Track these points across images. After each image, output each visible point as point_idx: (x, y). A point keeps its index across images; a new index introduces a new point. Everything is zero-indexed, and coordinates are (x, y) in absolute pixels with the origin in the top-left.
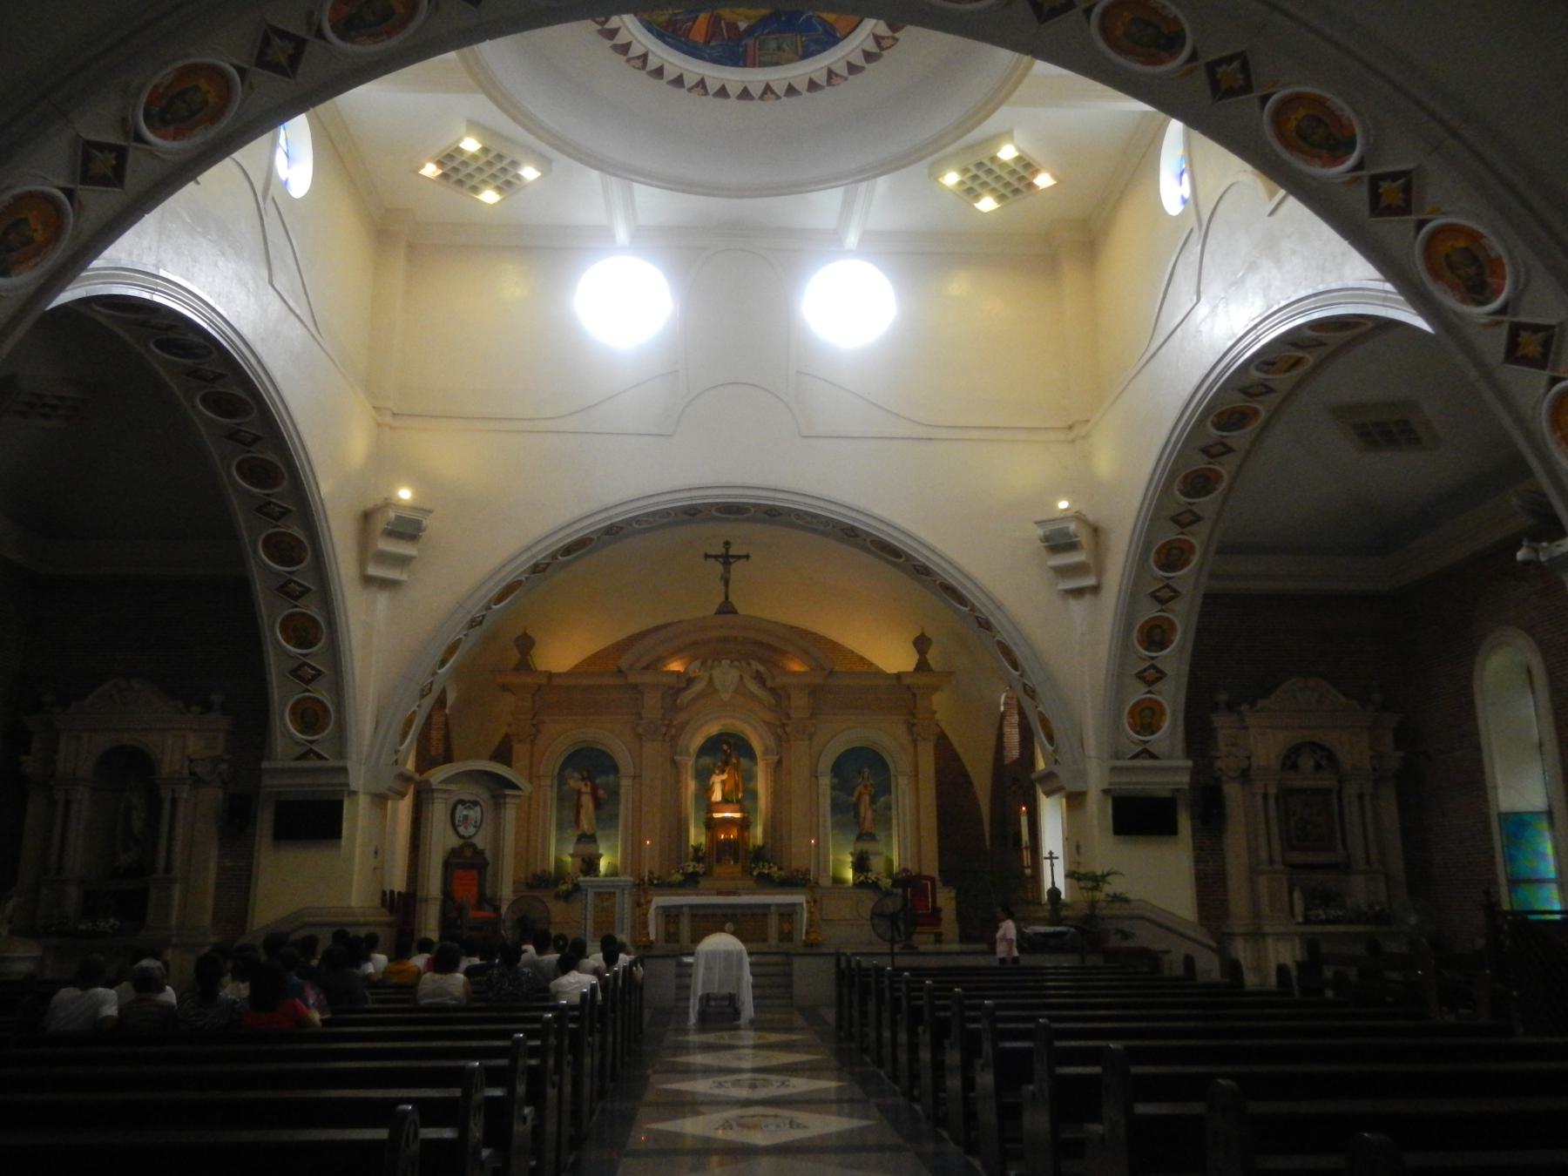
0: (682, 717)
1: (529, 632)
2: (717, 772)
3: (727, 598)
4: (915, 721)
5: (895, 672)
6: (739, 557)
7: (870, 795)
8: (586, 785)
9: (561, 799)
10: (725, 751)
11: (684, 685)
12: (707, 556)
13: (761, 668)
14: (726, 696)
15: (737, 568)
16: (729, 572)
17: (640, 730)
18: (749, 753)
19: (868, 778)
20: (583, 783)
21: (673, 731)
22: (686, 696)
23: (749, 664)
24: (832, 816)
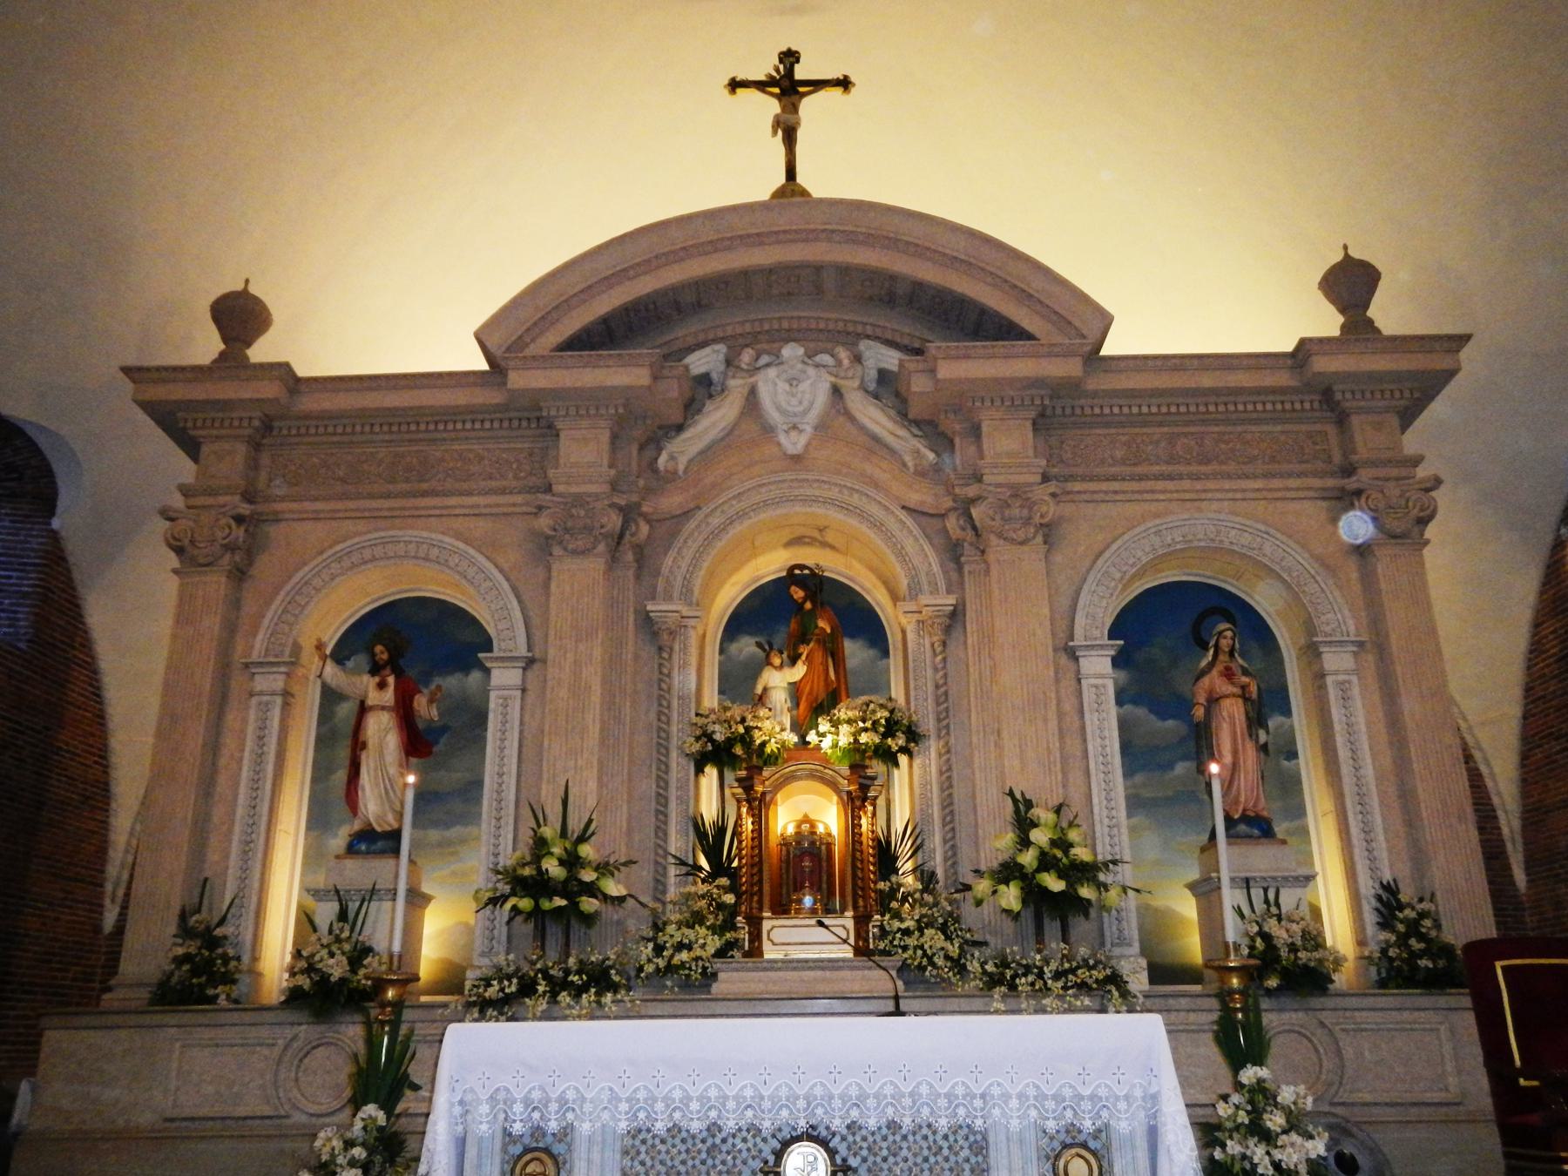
0: (671, 501)
1: (253, 290)
2: (777, 661)
3: (791, 173)
4: (1351, 483)
5: (1289, 347)
6: (818, 85)
7: (1246, 699)
8: (382, 686)
9: (324, 741)
10: (800, 606)
11: (680, 420)
12: (735, 85)
13: (891, 359)
14: (794, 443)
15: (810, 106)
16: (795, 109)
17: (544, 523)
18: (863, 622)
19: (1231, 654)
20: (377, 679)
21: (645, 529)
22: (683, 450)
23: (858, 359)
24: (1128, 773)
